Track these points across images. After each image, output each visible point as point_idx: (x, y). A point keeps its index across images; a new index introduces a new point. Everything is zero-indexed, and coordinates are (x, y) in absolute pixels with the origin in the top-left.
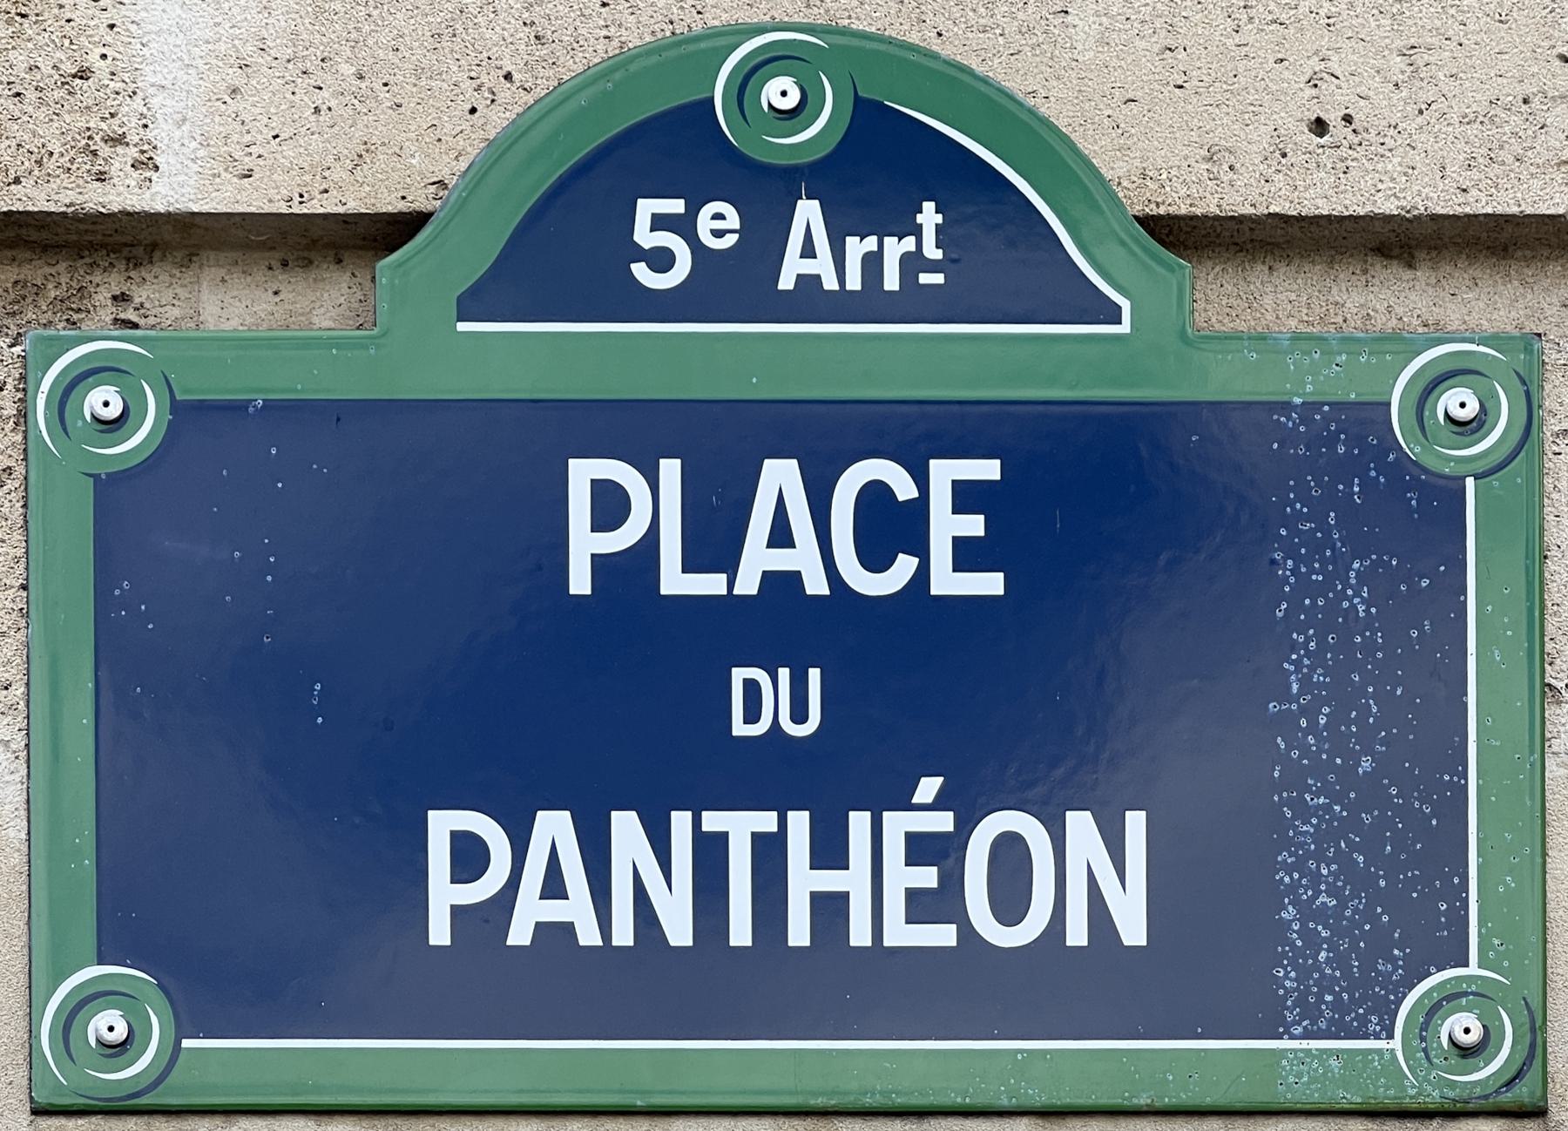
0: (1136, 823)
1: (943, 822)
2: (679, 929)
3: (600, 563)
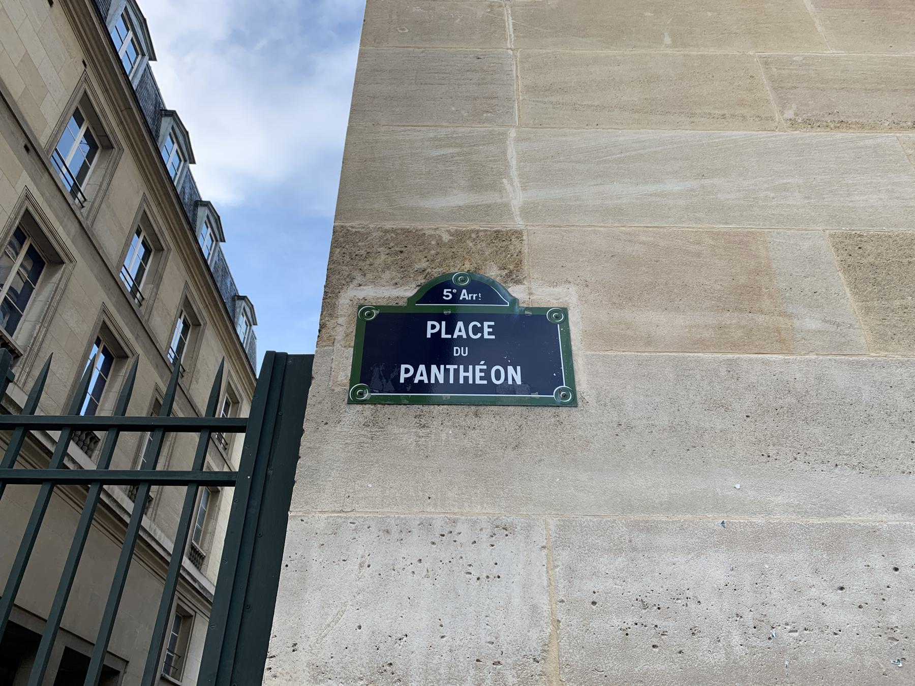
0: (519, 368)
1: (485, 367)
2: (441, 381)
3: (432, 334)
